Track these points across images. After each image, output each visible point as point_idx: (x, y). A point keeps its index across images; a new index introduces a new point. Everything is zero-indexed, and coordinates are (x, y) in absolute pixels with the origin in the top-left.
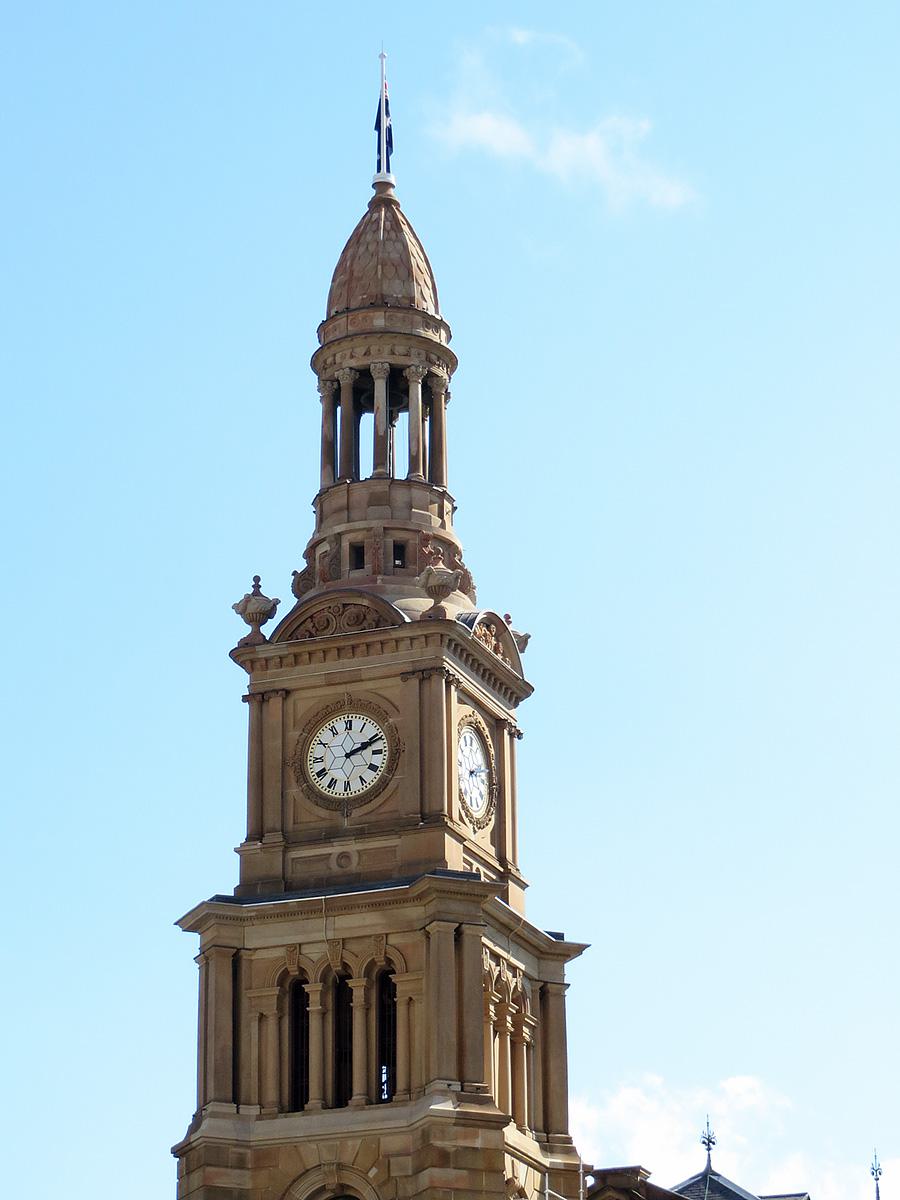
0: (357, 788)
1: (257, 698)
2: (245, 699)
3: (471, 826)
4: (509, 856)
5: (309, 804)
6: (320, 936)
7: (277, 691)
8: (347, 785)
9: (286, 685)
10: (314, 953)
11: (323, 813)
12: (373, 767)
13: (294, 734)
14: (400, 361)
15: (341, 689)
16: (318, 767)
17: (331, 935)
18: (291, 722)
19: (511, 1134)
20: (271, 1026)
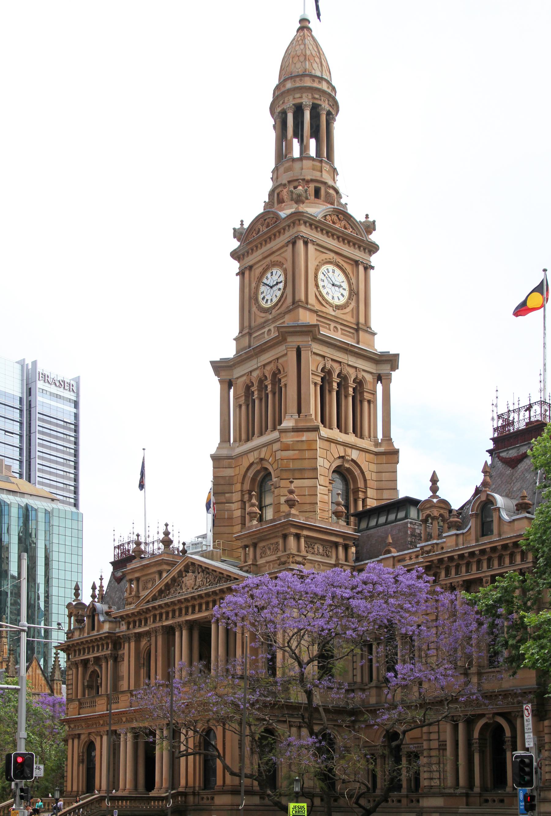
0: (275, 300)
1: (241, 273)
2: (237, 274)
3: (331, 309)
4: (362, 320)
5: (258, 313)
6: (255, 367)
7: (246, 268)
8: (271, 300)
9: (250, 263)
10: (255, 374)
11: (263, 315)
12: (279, 289)
13: (254, 285)
14: (298, 101)
15: (268, 259)
16: (262, 296)
17: (259, 365)
18: (252, 279)
19: (324, 432)
20: (243, 408)
